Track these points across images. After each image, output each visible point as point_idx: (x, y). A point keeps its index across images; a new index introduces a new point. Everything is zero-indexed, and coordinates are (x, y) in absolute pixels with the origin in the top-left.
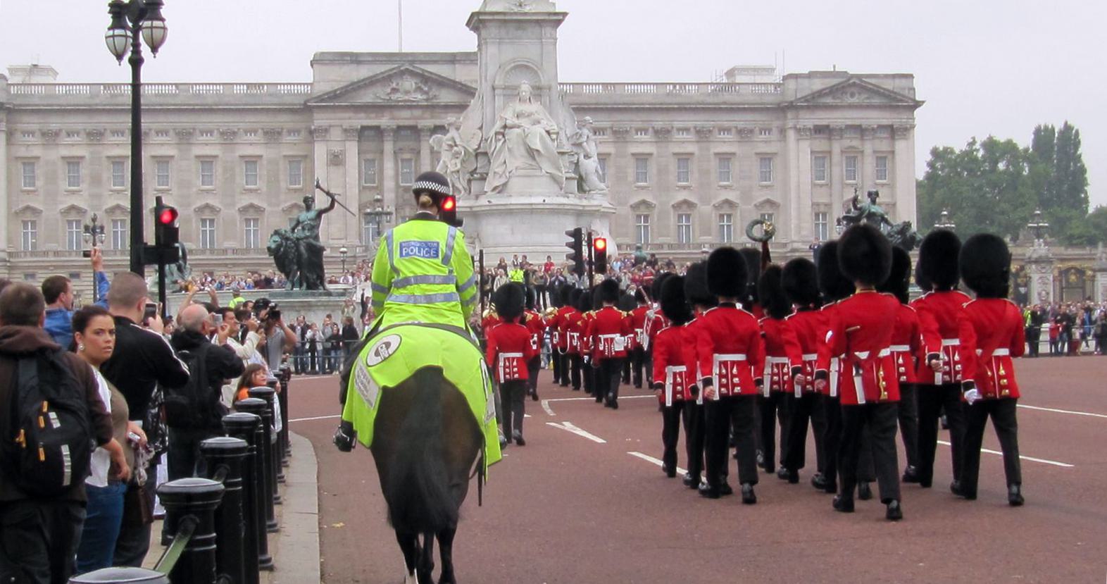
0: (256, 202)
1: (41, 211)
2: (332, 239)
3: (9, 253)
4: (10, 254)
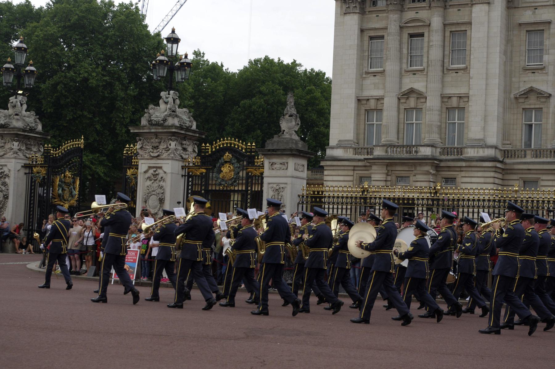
1: (550, 95)
3: (504, 151)
4: (506, 153)
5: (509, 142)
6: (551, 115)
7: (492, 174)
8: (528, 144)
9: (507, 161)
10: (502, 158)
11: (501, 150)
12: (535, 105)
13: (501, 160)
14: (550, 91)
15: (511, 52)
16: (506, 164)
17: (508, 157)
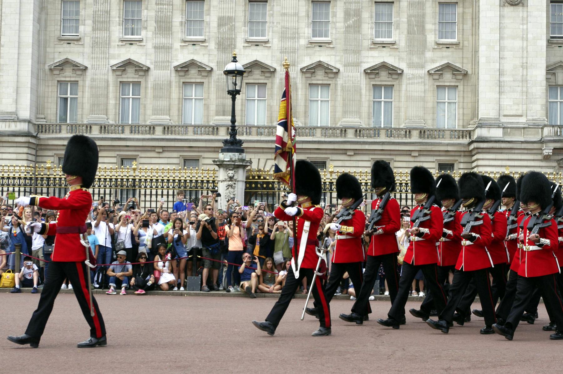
0: (391, 61)
1: (86, 68)
2: (505, 116)
3: (38, 125)
4: (41, 128)
5: (43, 116)
6: (87, 89)
7: (25, 150)
8: (64, 119)
9: (42, 136)
10: (36, 133)
11: (35, 124)
12: (70, 77)
13: (35, 134)
14: (86, 63)
15: (46, 20)
16: (39, 139)
17: (42, 132)
